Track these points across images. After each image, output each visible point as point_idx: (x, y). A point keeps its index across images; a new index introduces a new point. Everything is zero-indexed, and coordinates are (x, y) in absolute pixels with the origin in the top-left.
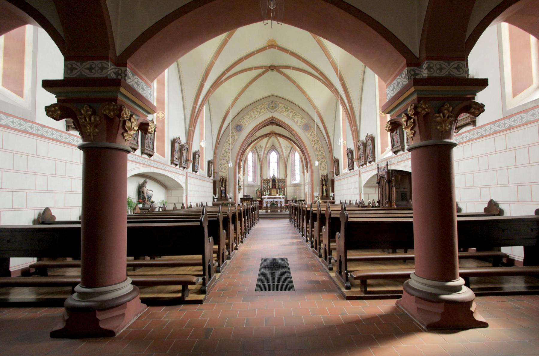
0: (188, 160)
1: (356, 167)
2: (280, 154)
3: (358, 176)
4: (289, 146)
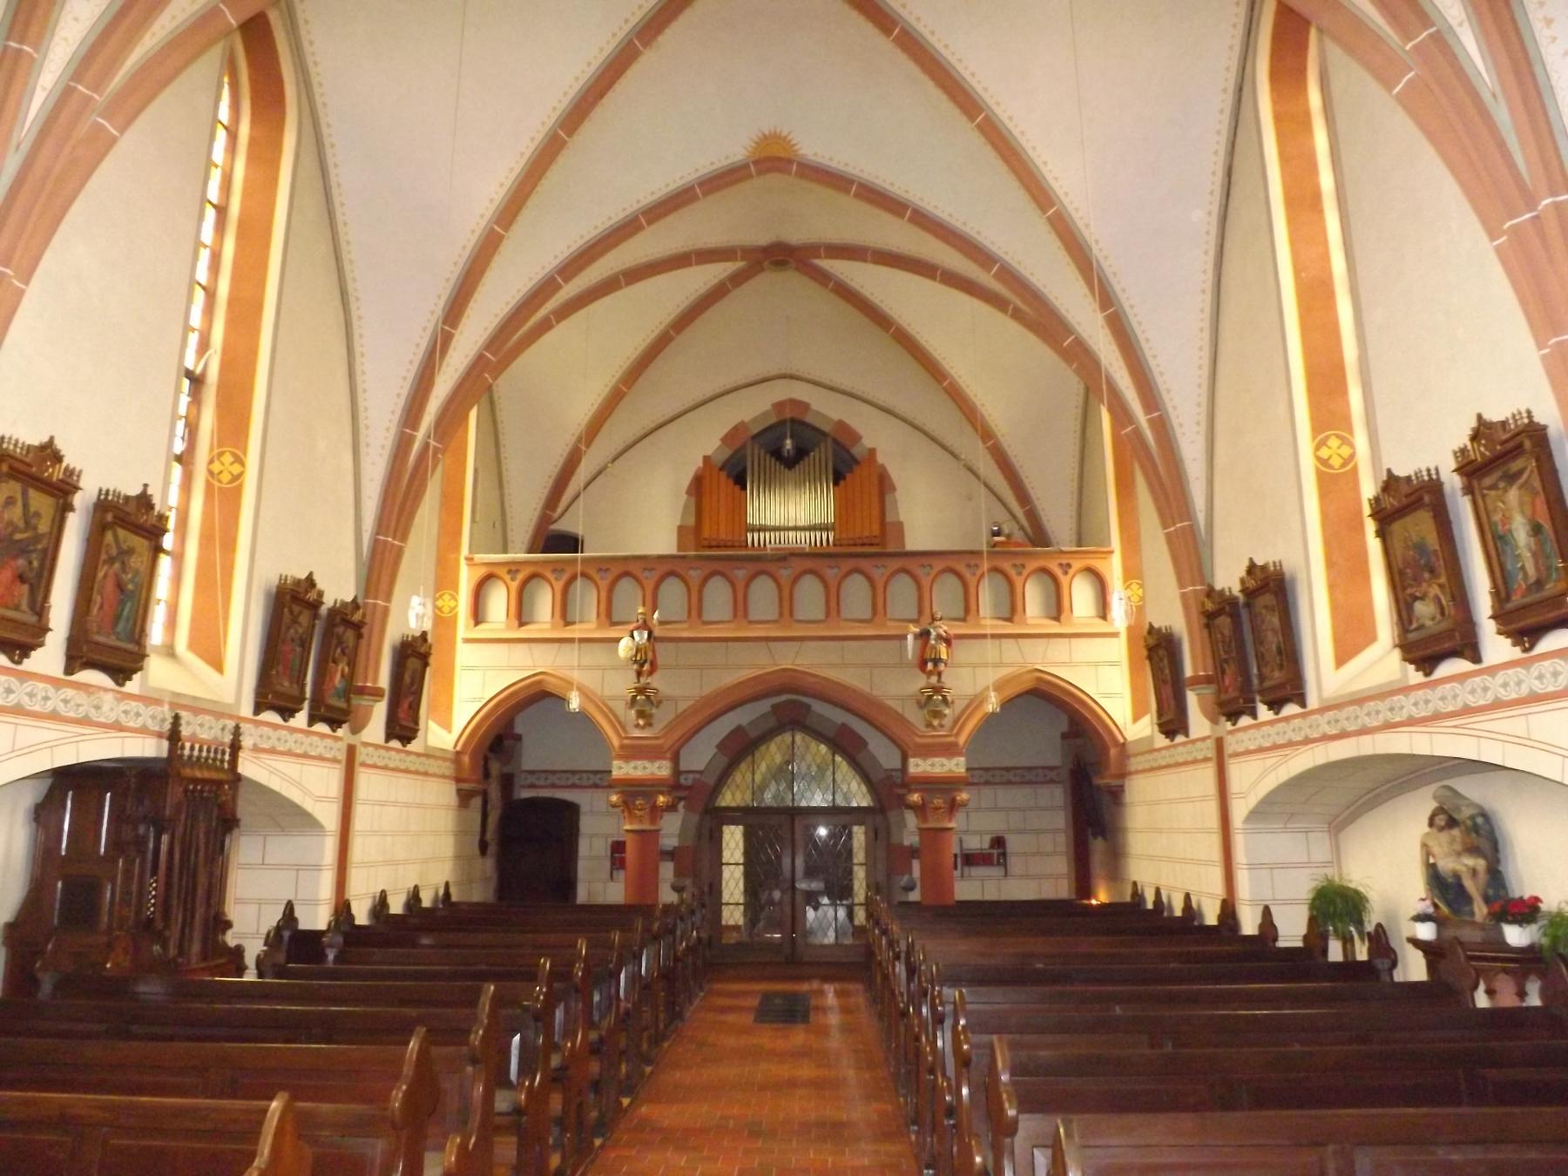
0: (362, 691)
1: (1199, 723)
3: (1208, 773)
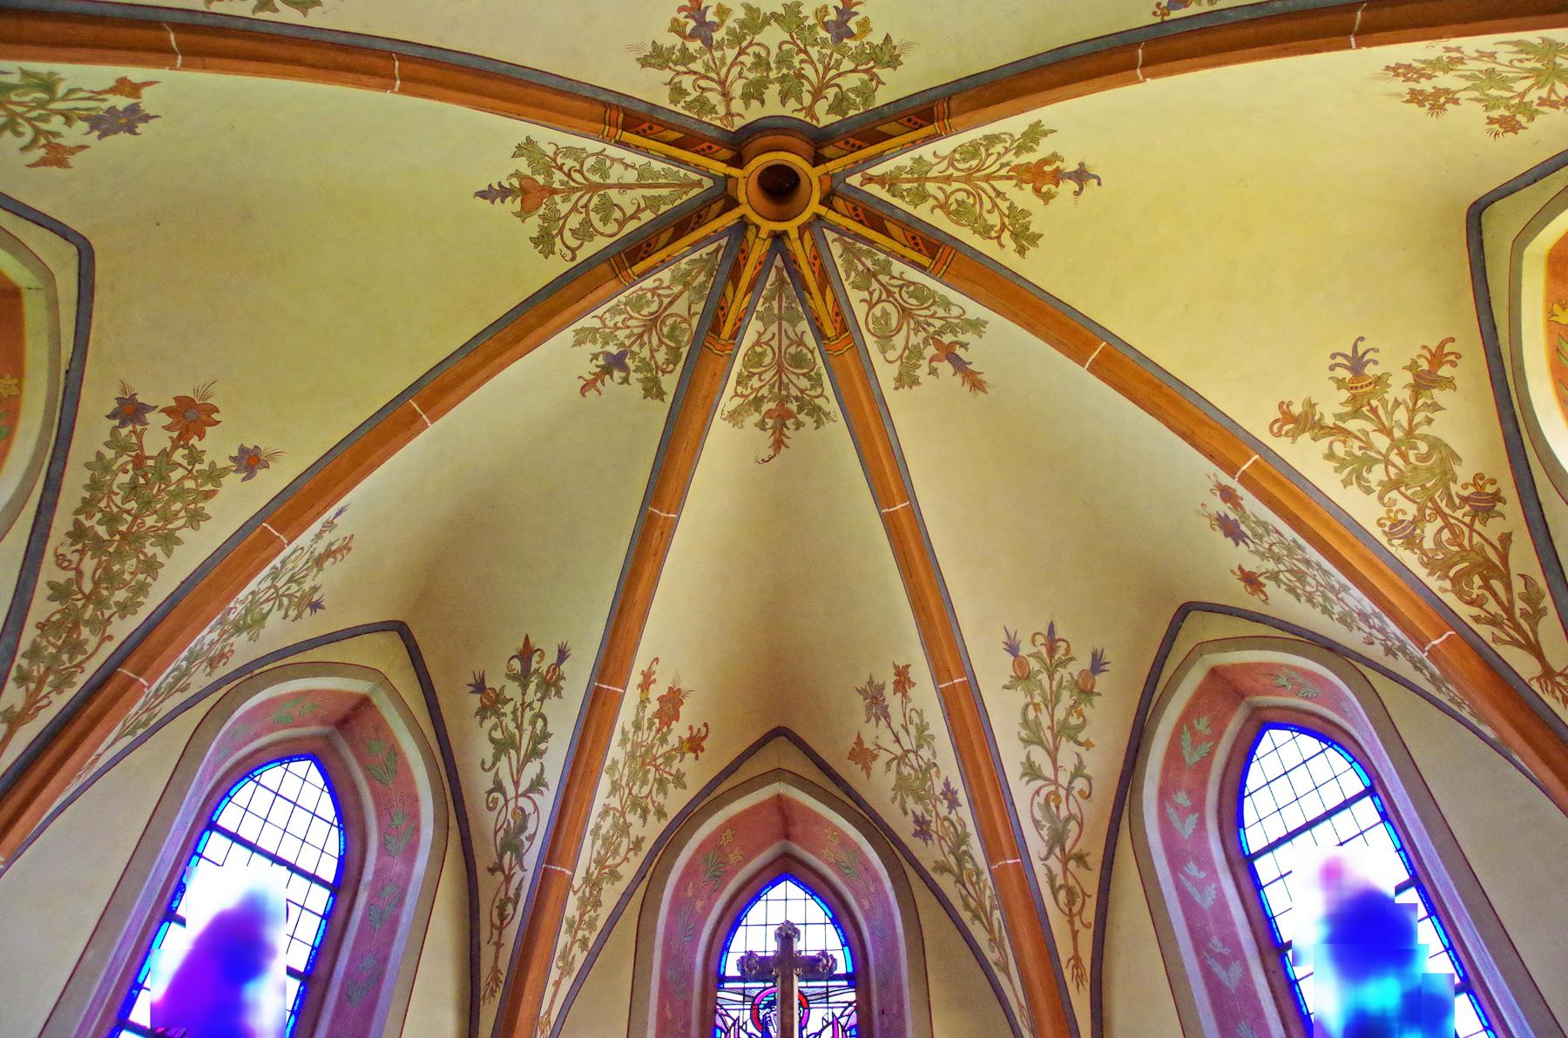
2: (928, 854)
4: (1097, 665)
